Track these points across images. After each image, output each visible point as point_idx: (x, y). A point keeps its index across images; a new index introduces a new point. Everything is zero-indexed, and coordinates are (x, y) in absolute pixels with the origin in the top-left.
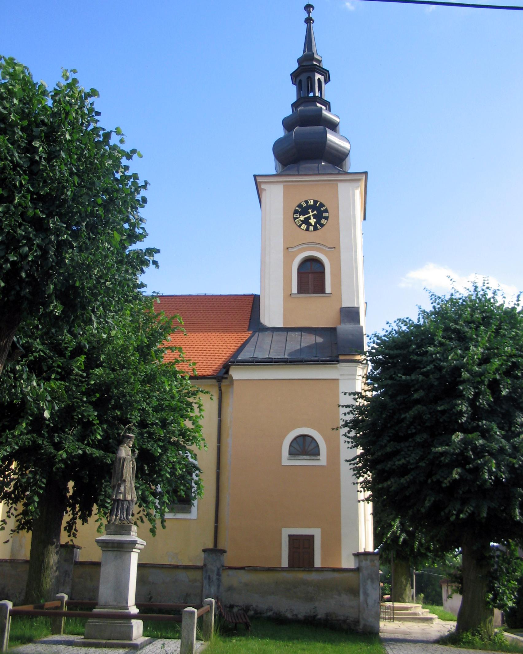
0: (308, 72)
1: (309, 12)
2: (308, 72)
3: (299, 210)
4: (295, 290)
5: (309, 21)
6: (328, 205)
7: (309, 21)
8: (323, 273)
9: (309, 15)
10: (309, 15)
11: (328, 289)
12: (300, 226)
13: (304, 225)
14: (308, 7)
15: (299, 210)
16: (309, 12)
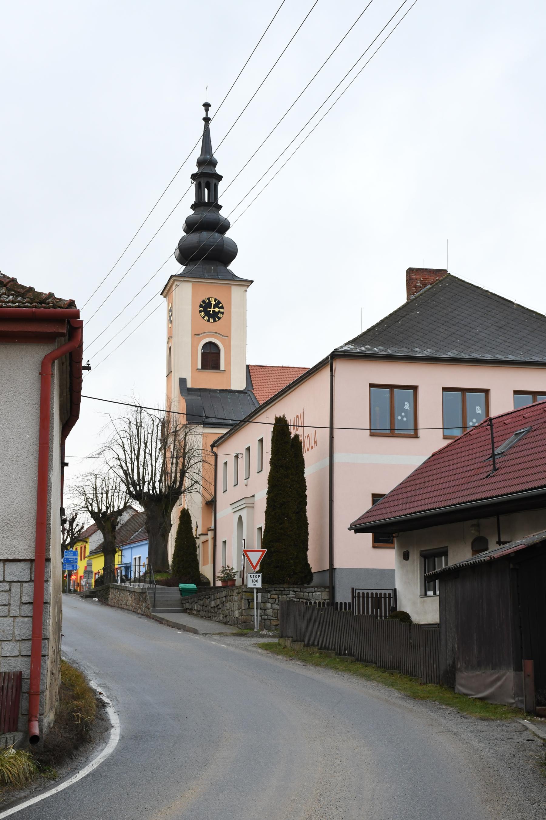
0: (207, 177)
1: (207, 110)
2: (207, 177)
3: (203, 304)
4: (200, 366)
5: (207, 120)
6: (224, 303)
7: (207, 120)
8: (218, 354)
9: (207, 114)
10: (207, 114)
11: (222, 367)
12: (203, 318)
14: (207, 106)
15: (203, 304)
16: (207, 110)
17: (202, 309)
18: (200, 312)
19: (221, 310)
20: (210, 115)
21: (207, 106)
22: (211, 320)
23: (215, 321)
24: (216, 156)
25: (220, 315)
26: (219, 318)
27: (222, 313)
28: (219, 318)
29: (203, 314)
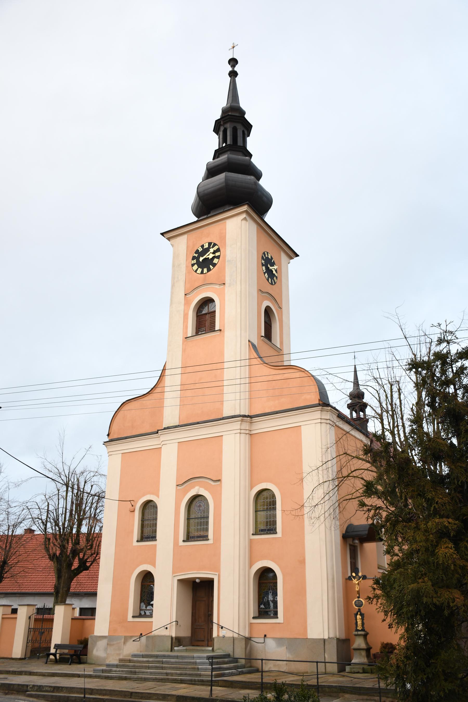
1: (233, 66)
3: (196, 255)
5: (233, 74)
7: (233, 74)
13: (199, 269)
14: (233, 62)
15: (196, 255)
16: (233, 66)
17: (195, 261)
18: (193, 265)
19: (217, 254)
20: (236, 69)
21: (233, 62)
22: (205, 270)
23: (209, 270)
24: (243, 105)
25: (216, 261)
26: (214, 265)
27: (218, 257)
28: (214, 265)
29: (196, 267)
